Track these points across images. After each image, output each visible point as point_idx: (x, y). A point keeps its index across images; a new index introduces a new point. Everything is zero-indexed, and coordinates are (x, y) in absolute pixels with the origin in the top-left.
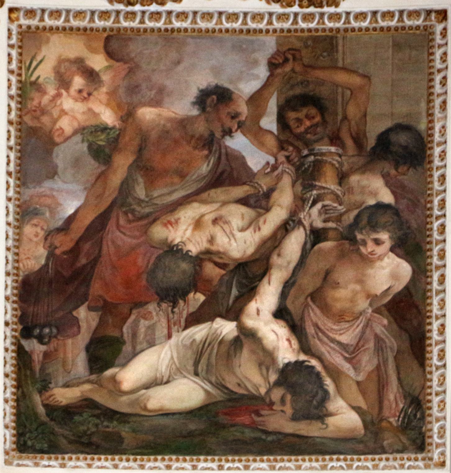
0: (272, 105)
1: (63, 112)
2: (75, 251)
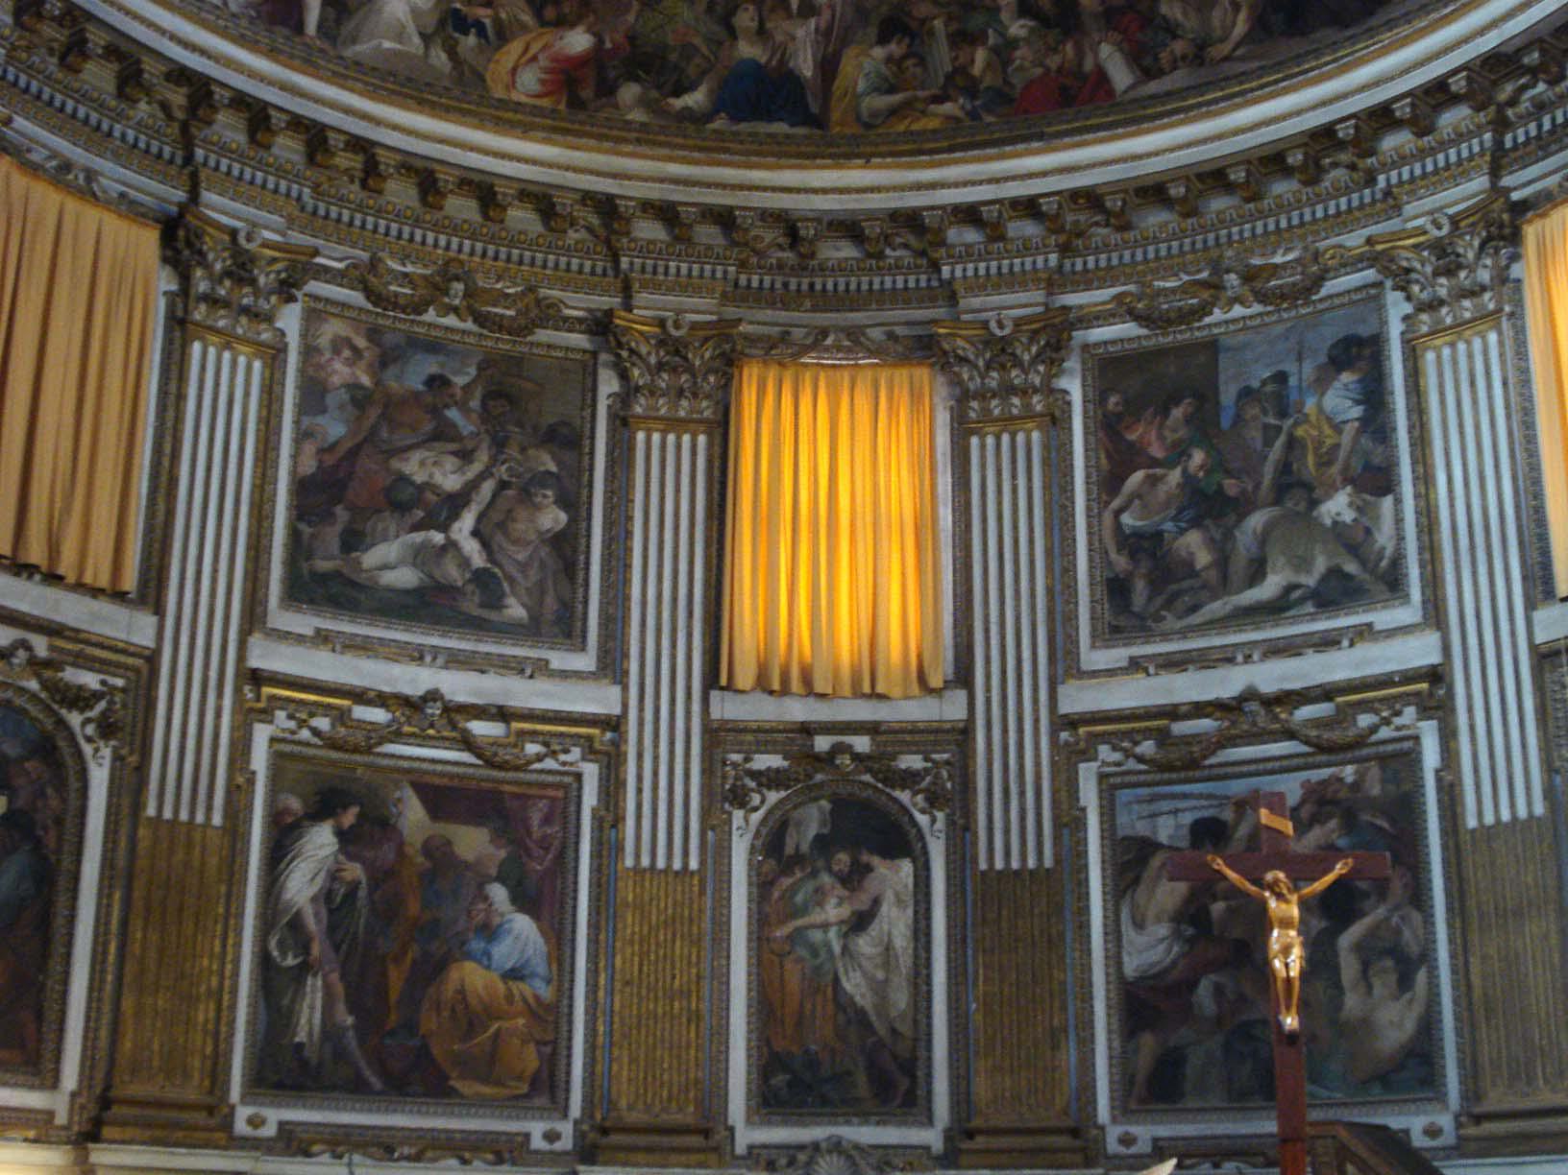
0: (478, 393)
1: (335, 372)
2: (337, 466)
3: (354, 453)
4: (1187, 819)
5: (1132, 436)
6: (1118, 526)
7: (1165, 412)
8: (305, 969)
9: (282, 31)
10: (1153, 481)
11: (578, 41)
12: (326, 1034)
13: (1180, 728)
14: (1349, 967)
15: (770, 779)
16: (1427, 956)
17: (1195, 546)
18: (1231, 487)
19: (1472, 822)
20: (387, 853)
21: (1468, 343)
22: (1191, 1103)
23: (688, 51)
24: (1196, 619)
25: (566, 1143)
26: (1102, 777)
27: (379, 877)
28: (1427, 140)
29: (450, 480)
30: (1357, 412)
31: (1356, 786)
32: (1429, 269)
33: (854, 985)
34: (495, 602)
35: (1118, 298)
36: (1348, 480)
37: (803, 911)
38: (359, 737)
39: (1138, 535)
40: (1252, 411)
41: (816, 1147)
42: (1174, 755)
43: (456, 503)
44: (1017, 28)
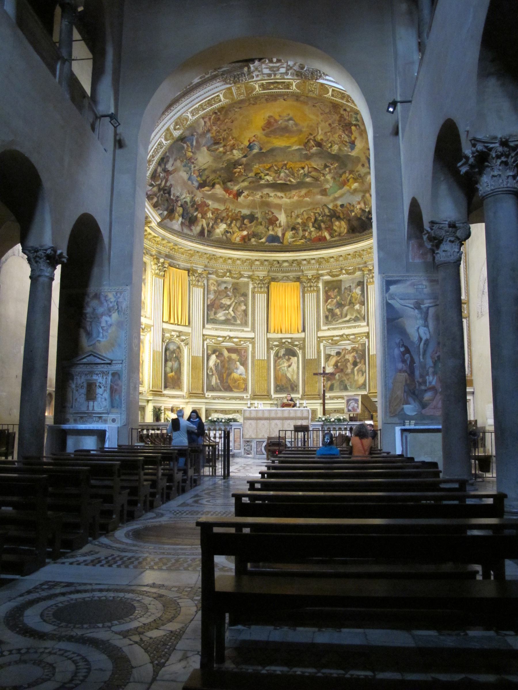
3: (215, 300)
4: (335, 351)
5: (329, 294)
6: (327, 308)
7: (334, 290)
8: (213, 375)
9: (202, 237)
10: (332, 301)
11: (245, 233)
12: (216, 383)
13: (335, 338)
14: (356, 373)
15: (276, 346)
16: (365, 372)
17: (337, 311)
18: (343, 302)
20: (223, 358)
22: (335, 391)
23: (262, 233)
24: (338, 322)
25: (249, 397)
26: (324, 345)
27: (222, 362)
29: (228, 303)
31: (358, 348)
33: (289, 375)
34: (236, 321)
35: (327, 272)
36: (359, 303)
37: (281, 364)
38: (218, 342)
39: (330, 309)
40: (346, 291)
41: (283, 398)
42: (333, 342)
43: (229, 306)
44: (312, 229)
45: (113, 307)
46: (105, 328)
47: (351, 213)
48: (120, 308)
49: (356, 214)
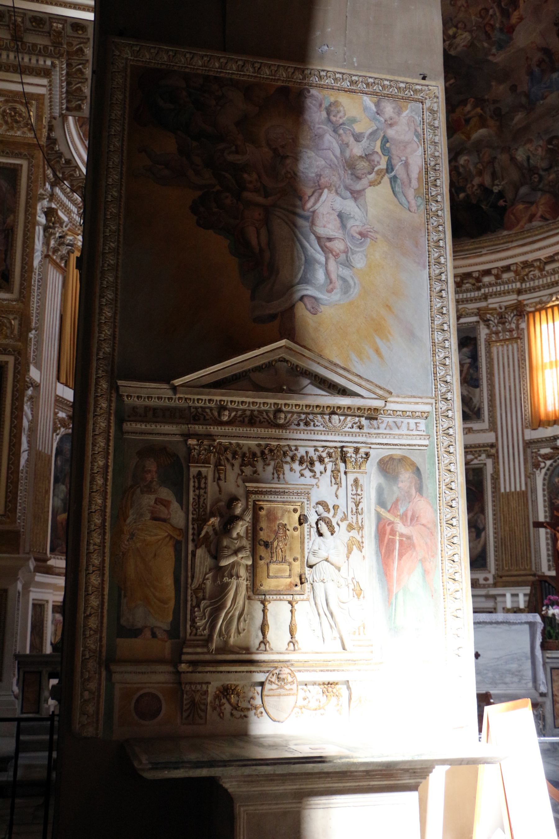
19: (502, 490)
21: (507, 346)
28: (499, 281)
30: (468, 361)
32: (496, 321)
45: (367, 157)
46: (337, 246)
47: (458, 195)
48: (399, 169)
49: (468, 196)
